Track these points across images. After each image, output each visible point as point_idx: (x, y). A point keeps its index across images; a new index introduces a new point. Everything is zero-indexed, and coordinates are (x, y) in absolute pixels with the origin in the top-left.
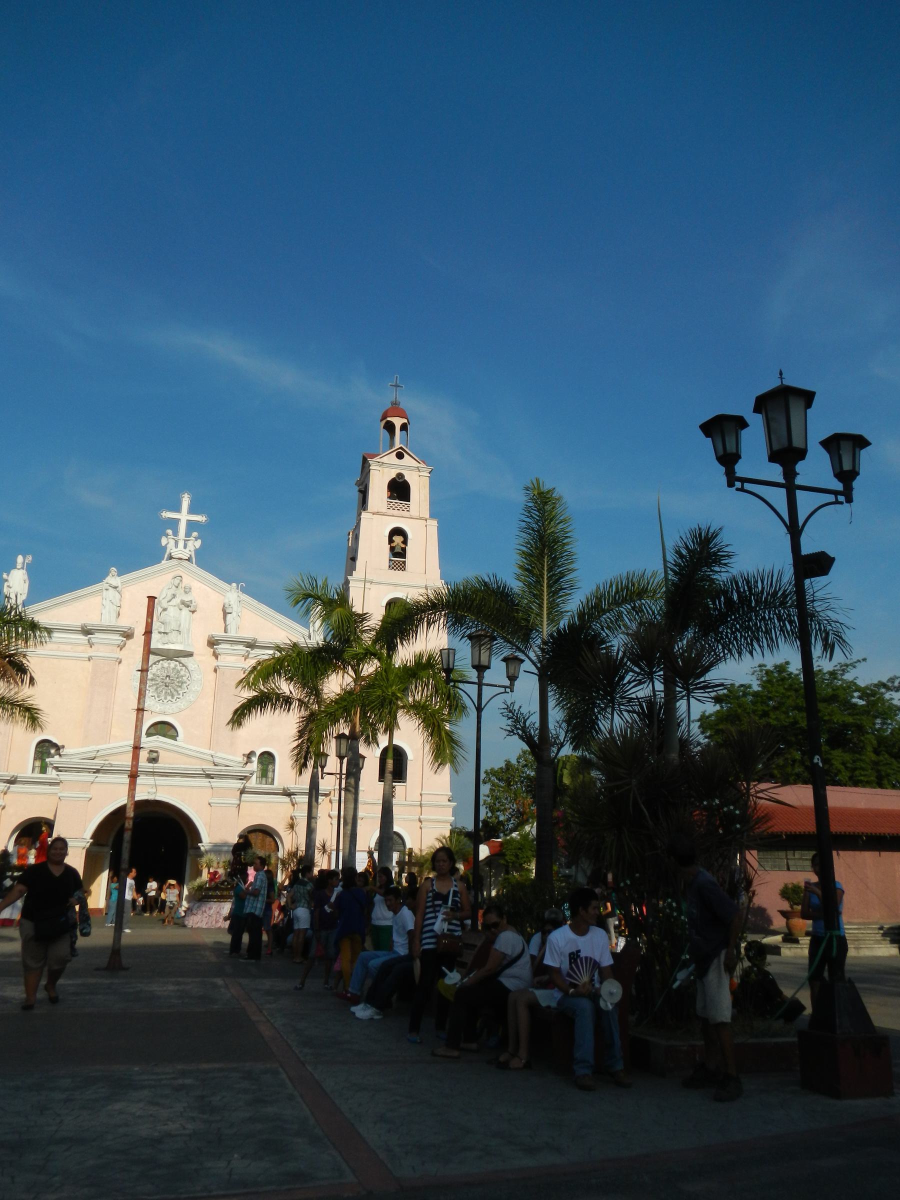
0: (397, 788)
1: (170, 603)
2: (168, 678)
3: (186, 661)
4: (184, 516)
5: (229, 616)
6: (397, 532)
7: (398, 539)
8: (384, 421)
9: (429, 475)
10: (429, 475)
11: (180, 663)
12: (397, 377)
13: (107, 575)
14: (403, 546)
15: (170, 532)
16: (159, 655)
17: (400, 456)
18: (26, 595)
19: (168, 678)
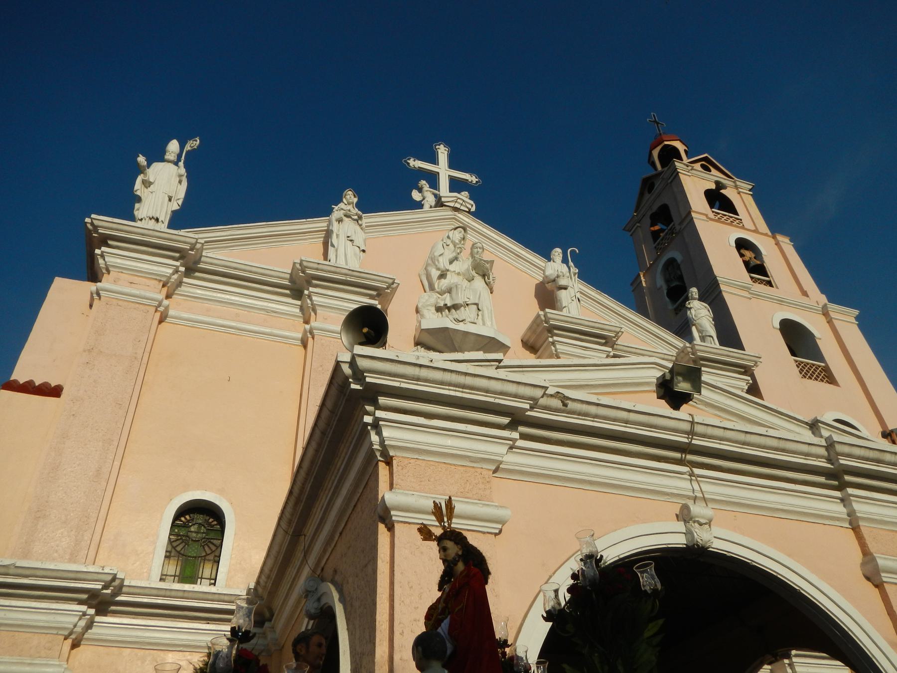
1: (452, 268)
4: (443, 169)
7: (749, 254)
8: (659, 148)
9: (751, 193)
10: (751, 193)
12: (654, 115)
13: (341, 201)
14: (759, 262)
15: (423, 183)
18: (180, 202)
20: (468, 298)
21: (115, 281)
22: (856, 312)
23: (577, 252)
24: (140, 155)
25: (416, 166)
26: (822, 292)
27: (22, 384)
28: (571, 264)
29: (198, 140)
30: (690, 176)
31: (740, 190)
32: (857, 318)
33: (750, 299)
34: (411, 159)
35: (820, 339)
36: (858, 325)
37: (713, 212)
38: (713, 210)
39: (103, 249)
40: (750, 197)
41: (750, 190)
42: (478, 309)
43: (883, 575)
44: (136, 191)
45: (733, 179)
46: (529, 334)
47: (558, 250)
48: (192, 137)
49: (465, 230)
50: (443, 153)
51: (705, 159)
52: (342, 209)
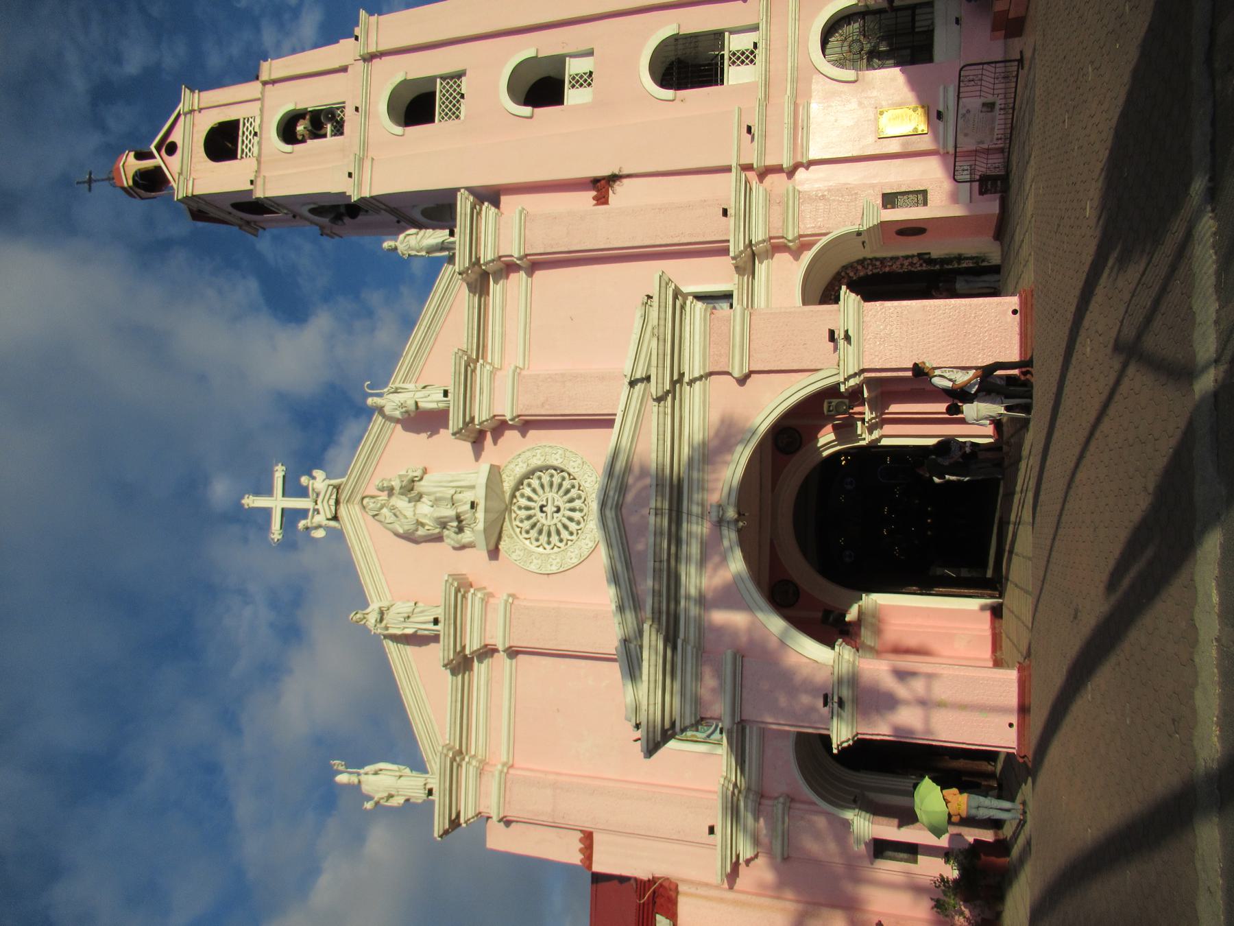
0: (734, 48)
2: (544, 509)
3: (512, 478)
4: (277, 503)
5: (425, 405)
6: (288, 131)
9: (197, 91)
10: (197, 91)
11: (517, 488)
14: (308, 117)
15: (302, 524)
16: (502, 528)
17: (172, 149)
19: (544, 509)
20: (447, 505)
21: (488, 807)
22: (363, 13)
23: (369, 383)
24: (365, 807)
25: (280, 532)
26: (338, 42)
27: (584, 855)
28: (386, 390)
29: (335, 762)
30: (194, 179)
31: (196, 108)
32: (371, 14)
33: (373, 159)
34: (272, 537)
35: (406, 73)
36: (380, 14)
37: (242, 158)
38: (239, 156)
39: (462, 820)
40: (201, 93)
41: (192, 91)
42: (455, 493)
43: (744, 372)
44: (399, 804)
45: (179, 115)
46: (470, 439)
47: (370, 401)
48: (331, 766)
49: (363, 498)
50: (252, 501)
51: (158, 148)
52: (375, 626)
